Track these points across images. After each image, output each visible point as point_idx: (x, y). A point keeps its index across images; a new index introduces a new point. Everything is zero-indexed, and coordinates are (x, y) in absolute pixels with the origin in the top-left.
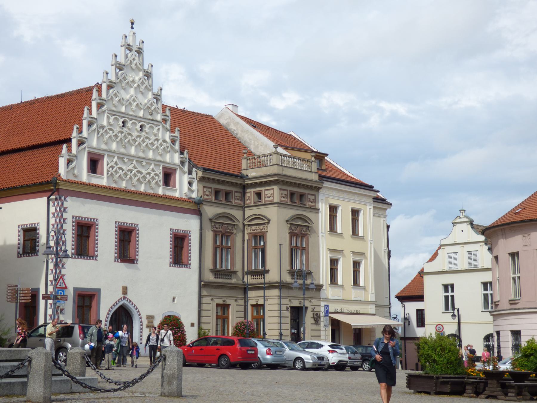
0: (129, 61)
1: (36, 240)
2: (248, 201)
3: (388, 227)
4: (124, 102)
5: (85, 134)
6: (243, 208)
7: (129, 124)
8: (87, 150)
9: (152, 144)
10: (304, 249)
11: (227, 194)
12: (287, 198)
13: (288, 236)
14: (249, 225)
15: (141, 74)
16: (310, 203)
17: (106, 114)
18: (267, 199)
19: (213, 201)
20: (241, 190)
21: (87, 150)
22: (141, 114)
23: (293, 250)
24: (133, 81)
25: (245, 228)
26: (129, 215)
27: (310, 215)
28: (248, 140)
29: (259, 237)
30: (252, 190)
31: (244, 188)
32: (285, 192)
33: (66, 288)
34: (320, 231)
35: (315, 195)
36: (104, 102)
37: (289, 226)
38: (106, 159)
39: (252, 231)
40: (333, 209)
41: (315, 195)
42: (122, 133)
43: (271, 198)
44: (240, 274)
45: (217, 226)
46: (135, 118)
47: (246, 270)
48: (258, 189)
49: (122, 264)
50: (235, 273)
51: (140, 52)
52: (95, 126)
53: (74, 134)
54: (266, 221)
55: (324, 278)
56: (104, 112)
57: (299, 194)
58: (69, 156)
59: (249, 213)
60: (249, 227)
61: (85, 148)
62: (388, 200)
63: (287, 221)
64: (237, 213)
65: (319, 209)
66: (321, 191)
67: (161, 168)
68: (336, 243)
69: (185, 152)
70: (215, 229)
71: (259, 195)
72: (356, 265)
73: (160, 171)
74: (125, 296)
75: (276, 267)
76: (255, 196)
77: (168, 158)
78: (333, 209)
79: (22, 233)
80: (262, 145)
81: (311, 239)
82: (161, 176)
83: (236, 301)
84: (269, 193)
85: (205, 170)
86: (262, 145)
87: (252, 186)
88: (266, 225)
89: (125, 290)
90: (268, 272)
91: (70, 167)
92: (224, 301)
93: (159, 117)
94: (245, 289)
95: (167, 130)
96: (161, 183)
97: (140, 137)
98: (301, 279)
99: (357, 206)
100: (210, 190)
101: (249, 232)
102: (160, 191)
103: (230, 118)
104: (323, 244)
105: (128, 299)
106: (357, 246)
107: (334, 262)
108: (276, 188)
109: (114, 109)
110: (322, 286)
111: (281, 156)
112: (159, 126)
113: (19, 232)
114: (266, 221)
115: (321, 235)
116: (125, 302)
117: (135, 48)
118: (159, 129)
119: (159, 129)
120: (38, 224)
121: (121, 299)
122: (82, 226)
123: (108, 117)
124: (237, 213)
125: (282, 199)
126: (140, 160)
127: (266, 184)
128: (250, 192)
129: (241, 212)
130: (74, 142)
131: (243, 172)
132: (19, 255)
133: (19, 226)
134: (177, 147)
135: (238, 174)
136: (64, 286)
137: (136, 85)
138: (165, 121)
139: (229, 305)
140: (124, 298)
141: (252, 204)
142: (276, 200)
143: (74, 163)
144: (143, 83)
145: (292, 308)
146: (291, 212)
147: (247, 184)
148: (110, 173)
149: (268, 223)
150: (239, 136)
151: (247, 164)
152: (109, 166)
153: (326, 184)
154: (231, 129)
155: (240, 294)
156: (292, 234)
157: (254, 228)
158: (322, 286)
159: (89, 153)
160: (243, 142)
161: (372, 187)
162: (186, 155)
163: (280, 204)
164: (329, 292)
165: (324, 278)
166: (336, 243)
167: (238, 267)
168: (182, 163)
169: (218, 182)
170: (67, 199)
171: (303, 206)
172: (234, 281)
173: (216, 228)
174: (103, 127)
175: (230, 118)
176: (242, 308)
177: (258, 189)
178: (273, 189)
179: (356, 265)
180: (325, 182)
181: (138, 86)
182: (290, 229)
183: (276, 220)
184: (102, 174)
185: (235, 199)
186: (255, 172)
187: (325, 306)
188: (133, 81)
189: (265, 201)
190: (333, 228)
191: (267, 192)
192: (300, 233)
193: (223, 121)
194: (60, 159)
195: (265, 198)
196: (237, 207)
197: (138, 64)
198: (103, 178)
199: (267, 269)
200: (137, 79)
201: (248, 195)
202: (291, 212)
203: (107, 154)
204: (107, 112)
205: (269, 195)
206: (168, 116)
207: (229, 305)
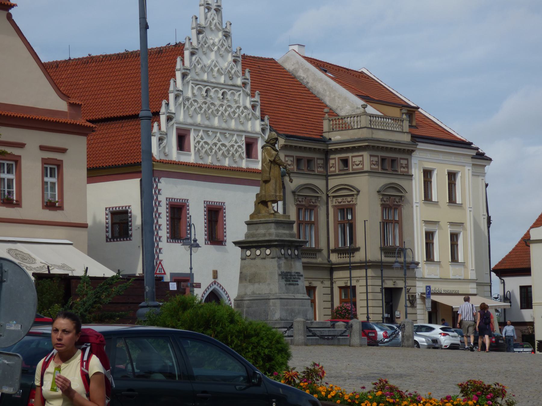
0: (209, 22)
1: (128, 223)
2: (332, 169)
3: (487, 185)
4: (206, 69)
5: (172, 108)
6: (326, 177)
7: (212, 93)
8: (175, 126)
9: (234, 112)
10: (397, 222)
11: (309, 161)
12: (378, 165)
13: (379, 208)
14: (334, 197)
15: (220, 35)
16: (402, 169)
17: (190, 85)
18: (355, 167)
19: (295, 171)
20: (323, 156)
21: (175, 126)
22: (222, 80)
23: (385, 224)
24: (214, 44)
25: (330, 200)
26: (215, 193)
27: (403, 183)
28: (321, 90)
29: (346, 210)
30: (337, 156)
31: (327, 153)
32: (375, 159)
33: (165, 274)
34: (414, 201)
35: (407, 159)
36: (188, 71)
37: (381, 197)
38: (192, 135)
39: (337, 204)
40: (427, 174)
41: (407, 159)
42: (205, 103)
43: (360, 166)
44: (325, 252)
45: (300, 200)
46: (217, 86)
47: (332, 246)
48: (344, 155)
49: (212, 246)
50: (320, 251)
51: (218, 10)
52: (181, 99)
53: (163, 110)
54: (355, 192)
55: (420, 254)
56: (188, 82)
57: (391, 160)
58: (160, 134)
59: (333, 182)
60: (334, 199)
61: (173, 125)
62: (487, 155)
63: (378, 192)
64: (320, 183)
65: (412, 175)
66: (414, 154)
67: (243, 139)
68: (431, 213)
69: (266, 118)
70: (298, 203)
71: (345, 162)
72: (454, 237)
73: (242, 142)
74: (216, 280)
75: (369, 246)
76: (341, 163)
77: (249, 126)
78: (427, 174)
79: (109, 216)
80: (344, 101)
81: (405, 211)
82: (244, 147)
83: (322, 282)
84: (357, 160)
85: (288, 137)
86: (344, 101)
87: (336, 151)
88: (355, 197)
89: (215, 274)
90: (358, 249)
91: (162, 146)
92: (310, 283)
93: (239, 82)
94: (331, 269)
95: (248, 95)
96: (244, 155)
97: (222, 105)
98: (395, 257)
99: (453, 169)
100: (292, 159)
101: (334, 204)
102: (244, 164)
103: (298, 63)
104: (418, 214)
105: (218, 284)
106: (454, 215)
107: (429, 235)
108: (366, 154)
109: (197, 78)
110: (417, 264)
111: (370, 116)
112: (240, 91)
113: (107, 214)
114: (355, 192)
115: (415, 205)
116: (215, 286)
117: (214, 7)
118: (240, 95)
119: (240, 95)
120: (129, 207)
121: (212, 283)
122: (174, 208)
123: (193, 88)
124: (320, 183)
125: (373, 166)
126: (224, 131)
127: (354, 149)
128: (334, 159)
129: (324, 182)
130: (163, 118)
131: (325, 135)
132: (108, 240)
133: (106, 209)
134: (258, 113)
135: (319, 137)
136: (163, 272)
137: (216, 48)
138: (244, 84)
139: (314, 288)
140: (215, 282)
141: (337, 172)
142: (367, 168)
143: (165, 141)
144: (223, 45)
145: (386, 289)
146: (382, 181)
147: (331, 149)
148: (197, 149)
149: (357, 195)
150: (310, 85)
151: (329, 125)
152: (196, 141)
153: (421, 146)
154: (300, 76)
155: (326, 275)
156: (385, 207)
157: (340, 199)
158: (417, 264)
159: (177, 129)
160: (315, 93)
161: (470, 144)
162: (267, 121)
163: (371, 172)
164: (425, 270)
165: (420, 254)
166: (431, 213)
167: (323, 245)
168: (263, 130)
169: (300, 149)
170: (160, 180)
171: (395, 173)
172: (319, 260)
173: (300, 202)
174: (188, 99)
175: (298, 63)
176: (328, 291)
177: (344, 155)
178: (362, 156)
179: (454, 237)
180: (419, 144)
181: (219, 48)
182: (382, 200)
183: (367, 190)
184: (189, 150)
185: (318, 167)
186: (340, 135)
187: (427, 287)
188: (214, 44)
189: (353, 169)
190: (427, 197)
191: (354, 159)
192: (393, 203)
193: (289, 66)
194: (152, 137)
195: (353, 165)
196: (319, 175)
197: (217, 24)
198: (190, 155)
199: (357, 246)
200: (217, 40)
201: (332, 162)
202: (382, 181)
203: (193, 128)
204: (191, 82)
205: (357, 163)
206: (248, 79)
207: (314, 288)
